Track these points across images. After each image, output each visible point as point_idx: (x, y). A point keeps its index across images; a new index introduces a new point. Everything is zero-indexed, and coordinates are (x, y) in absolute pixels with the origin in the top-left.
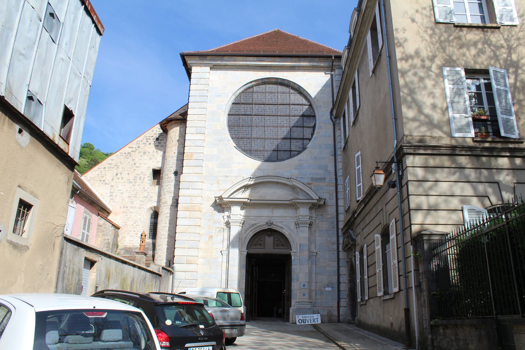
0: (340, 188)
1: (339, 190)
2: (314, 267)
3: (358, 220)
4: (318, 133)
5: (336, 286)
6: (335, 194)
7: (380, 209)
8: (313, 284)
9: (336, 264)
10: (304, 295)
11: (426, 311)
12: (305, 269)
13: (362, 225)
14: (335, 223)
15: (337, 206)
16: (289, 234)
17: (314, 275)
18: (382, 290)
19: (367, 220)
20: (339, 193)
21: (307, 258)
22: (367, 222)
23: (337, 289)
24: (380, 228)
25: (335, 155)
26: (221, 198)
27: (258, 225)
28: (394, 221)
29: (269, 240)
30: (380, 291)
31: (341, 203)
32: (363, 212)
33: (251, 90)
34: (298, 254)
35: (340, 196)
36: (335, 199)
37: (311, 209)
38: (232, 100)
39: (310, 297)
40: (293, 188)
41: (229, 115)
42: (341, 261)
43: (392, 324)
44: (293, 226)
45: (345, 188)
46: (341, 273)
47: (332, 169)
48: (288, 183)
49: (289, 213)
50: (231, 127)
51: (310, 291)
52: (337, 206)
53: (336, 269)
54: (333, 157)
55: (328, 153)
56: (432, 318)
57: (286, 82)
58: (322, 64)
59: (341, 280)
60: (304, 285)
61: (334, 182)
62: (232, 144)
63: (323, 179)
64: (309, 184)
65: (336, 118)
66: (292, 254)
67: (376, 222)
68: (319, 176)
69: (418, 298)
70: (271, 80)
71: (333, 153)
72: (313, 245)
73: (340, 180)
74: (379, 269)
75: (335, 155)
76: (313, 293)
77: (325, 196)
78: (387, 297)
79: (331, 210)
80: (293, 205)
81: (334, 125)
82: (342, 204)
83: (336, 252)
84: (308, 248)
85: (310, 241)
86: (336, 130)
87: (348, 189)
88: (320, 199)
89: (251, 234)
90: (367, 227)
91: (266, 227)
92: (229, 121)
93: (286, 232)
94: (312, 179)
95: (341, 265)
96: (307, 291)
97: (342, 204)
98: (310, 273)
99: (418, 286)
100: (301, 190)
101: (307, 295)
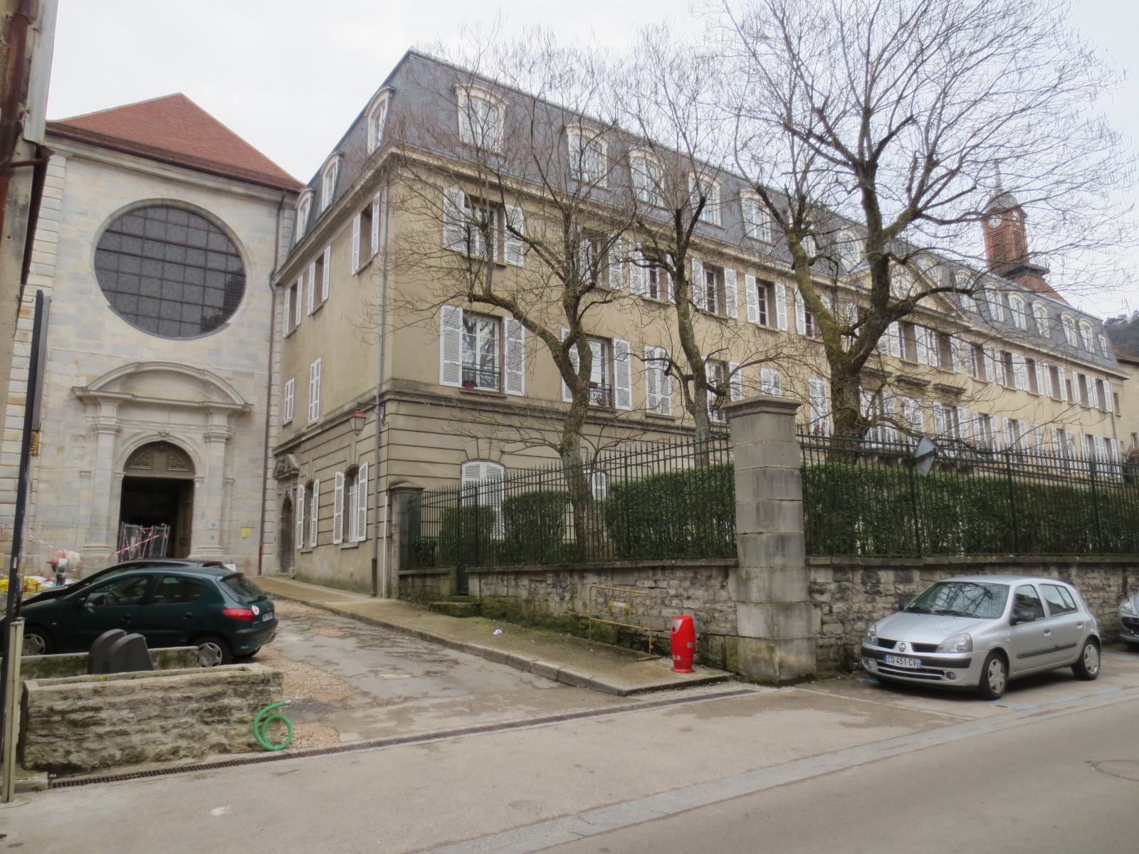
0: (275, 390)
1: (272, 392)
2: (229, 499)
3: (307, 446)
4: (248, 303)
5: (259, 526)
6: (266, 397)
7: (346, 443)
8: (226, 524)
9: (260, 496)
10: (213, 538)
11: (395, 563)
12: (217, 502)
13: (314, 454)
14: (263, 440)
15: (268, 415)
16: (194, 451)
17: (227, 510)
18: (341, 537)
19: (323, 450)
20: (272, 398)
21: (220, 486)
22: (324, 452)
23: (259, 529)
24: (345, 467)
25: (271, 341)
26: (83, 389)
27: (144, 435)
28: (366, 464)
29: (159, 458)
30: (337, 537)
31: (274, 411)
32: (318, 438)
33: (142, 213)
34: (206, 480)
35: (274, 401)
36: (266, 405)
37: (230, 416)
38: (106, 226)
39: (221, 542)
40: (205, 384)
41: (98, 249)
42: (268, 492)
43: (352, 575)
44: (199, 438)
45: (283, 394)
46: (267, 508)
47: (264, 359)
48: (197, 375)
49: (198, 420)
50: (99, 268)
51: (222, 532)
52: (268, 415)
53: (261, 502)
54: (268, 344)
55: (260, 337)
56: (402, 567)
57: (203, 213)
58: (265, 196)
59: (267, 517)
60: (213, 525)
61: (267, 379)
62: (103, 301)
63: (251, 375)
64: (229, 379)
65: (278, 285)
66: (196, 480)
67: (340, 456)
68: (244, 370)
69: (389, 549)
70: (177, 204)
71: (268, 337)
72: (229, 469)
73: (276, 378)
74: (338, 513)
75: (271, 341)
76: (226, 536)
77: (252, 400)
78: (346, 546)
79: (259, 419)
80: (205, 410)
81: (274, 295)
82: (276, 413)
83: (262, 480)
84: (221, 472)
85: (227, 462)
86: (278, 301)
87: (290, 397)
88: (246, 405)
89: (132, 449)
90: (323, 459)
91: (160, 439)
92: (97, 260)
93: (188, 448)
94: (235, 373)
95: (267, 498)
96: (218, 532)
97: (276, 413)
98: (223, 507)
99: (390, 537)
100: (218, 387)
101: (217, 539)
